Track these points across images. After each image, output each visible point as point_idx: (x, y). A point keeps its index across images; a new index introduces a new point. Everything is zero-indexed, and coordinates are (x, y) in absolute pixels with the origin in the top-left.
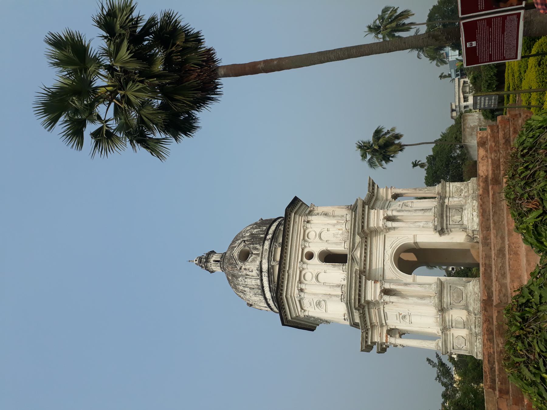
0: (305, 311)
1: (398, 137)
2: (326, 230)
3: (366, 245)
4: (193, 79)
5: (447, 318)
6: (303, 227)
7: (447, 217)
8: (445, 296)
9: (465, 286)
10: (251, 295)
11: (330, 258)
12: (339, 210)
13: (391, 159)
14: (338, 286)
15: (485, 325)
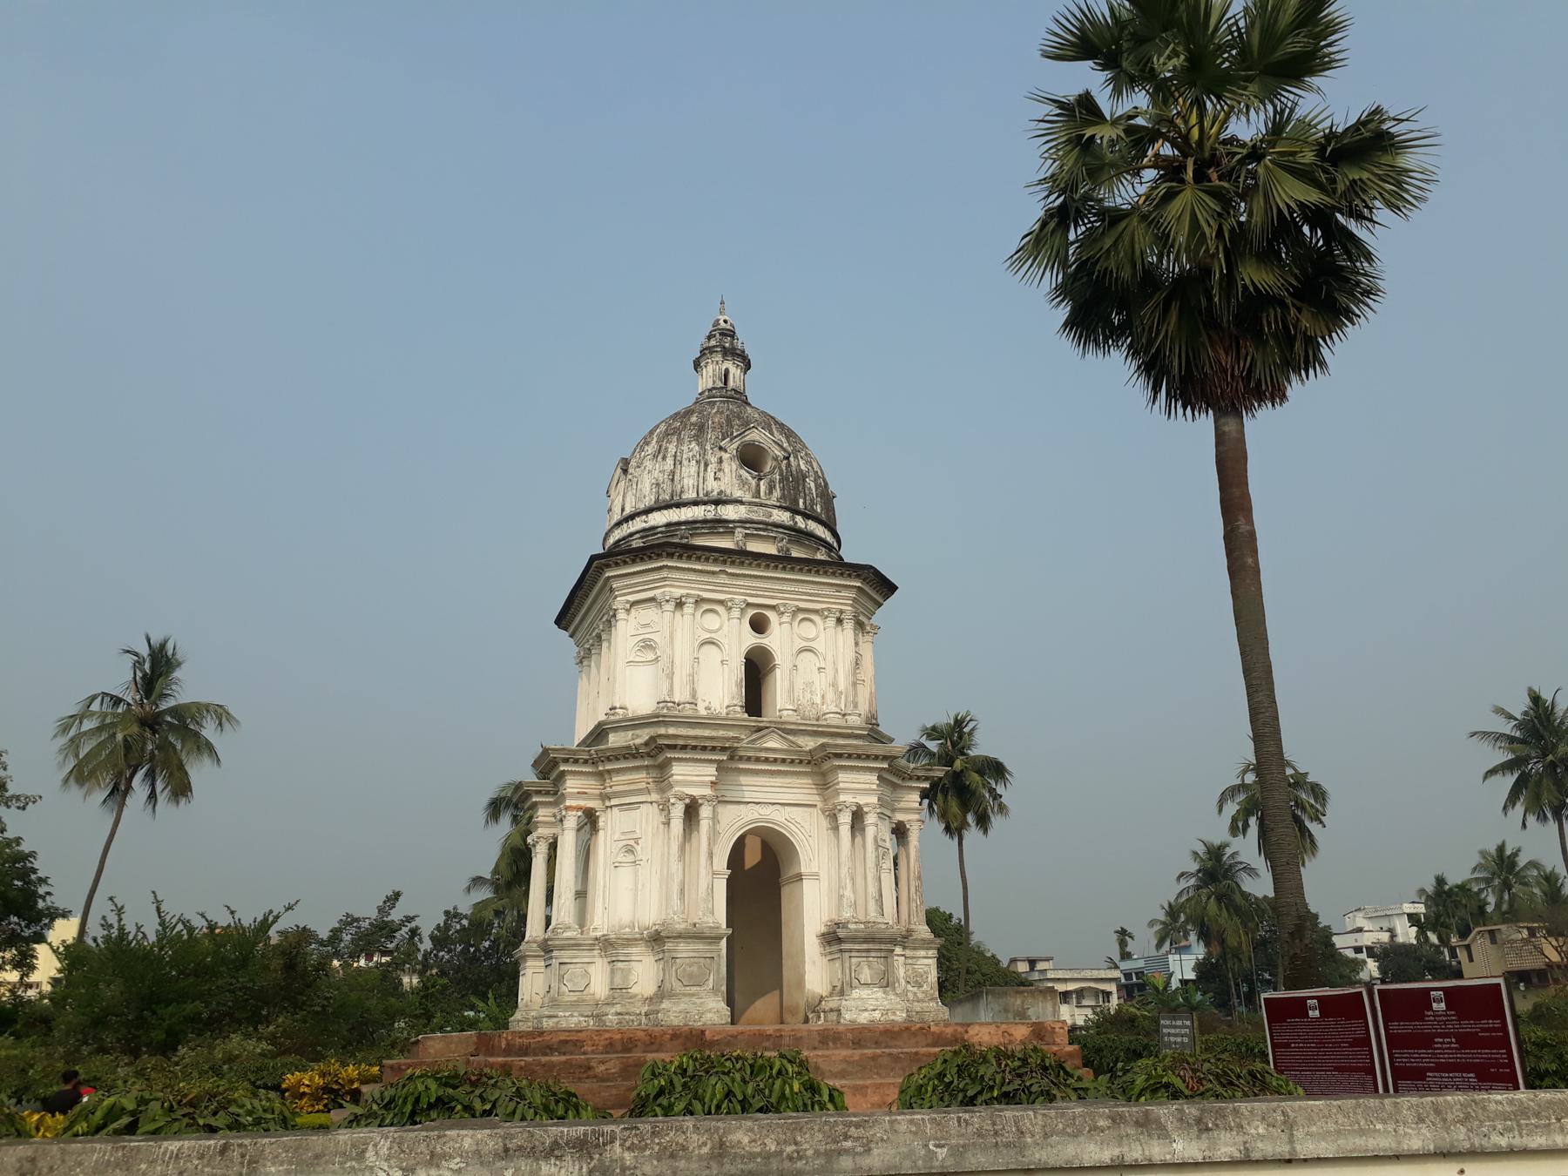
0: (628, 611)
1: (983, 821)
2: (823, 665)
3: (792, 761)
4: (1216, 356)
5: (634, 950)
6: (829, 610)
7: (868, 951)
9: (715, 991)
11: (757, 670)
12: (867, 696)
13: (926, 801)
14: (694, 694)
15: (641, 1035)
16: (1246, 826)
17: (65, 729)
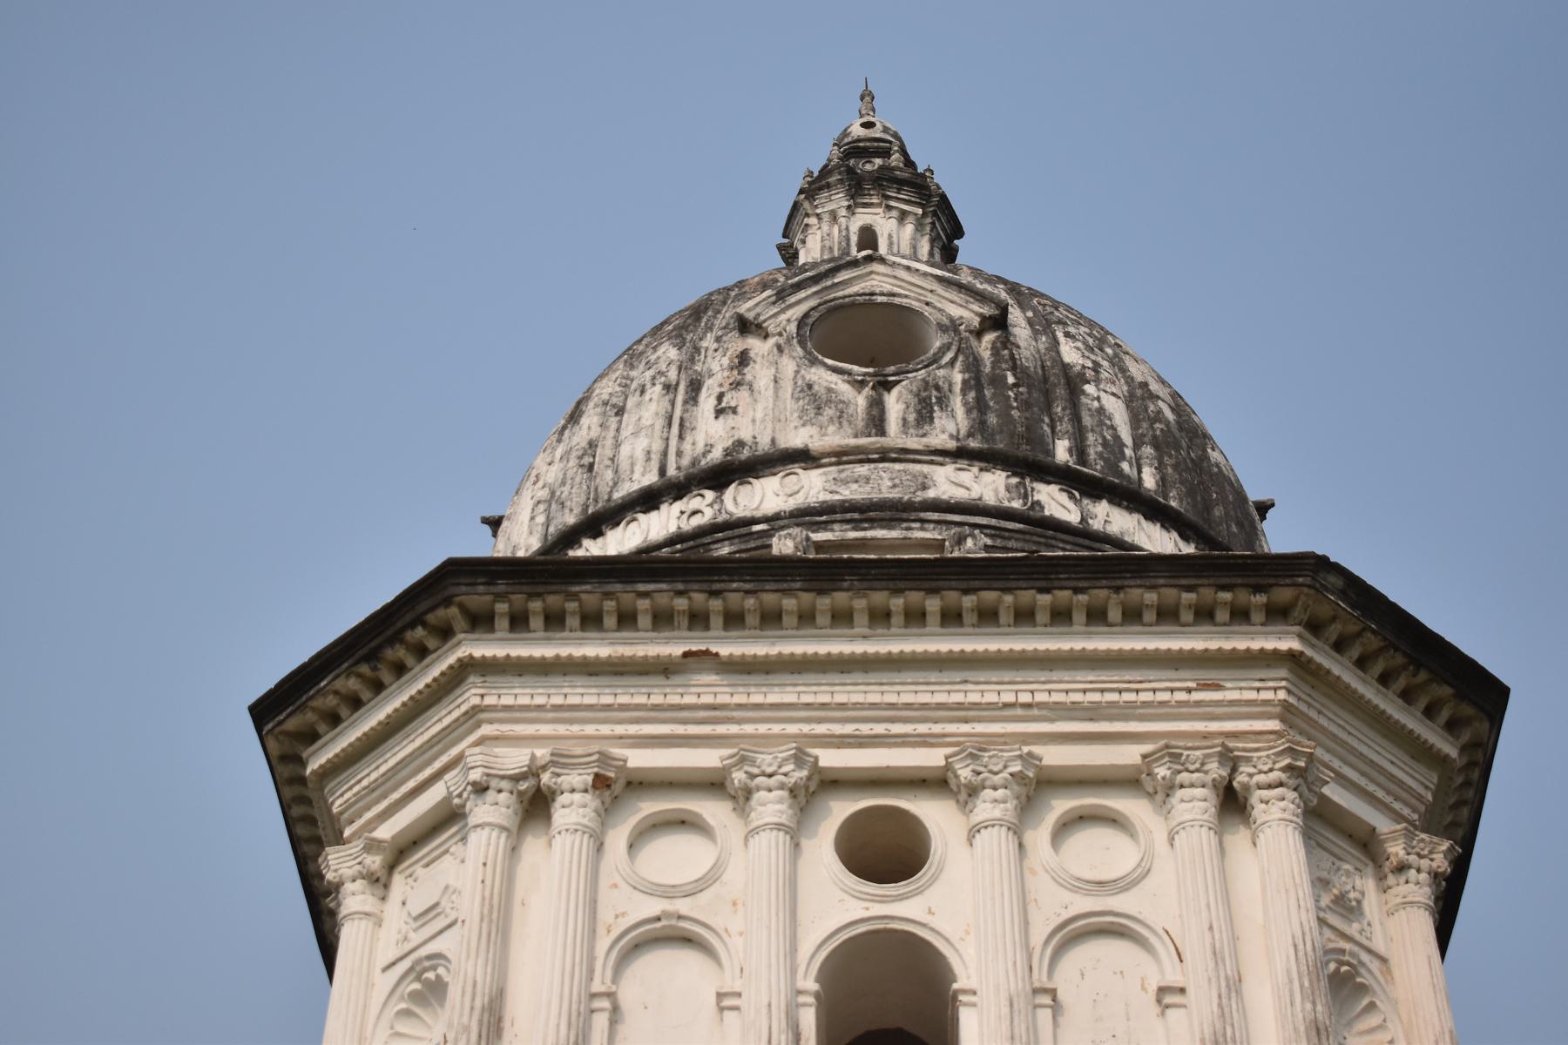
10: (552, 475)
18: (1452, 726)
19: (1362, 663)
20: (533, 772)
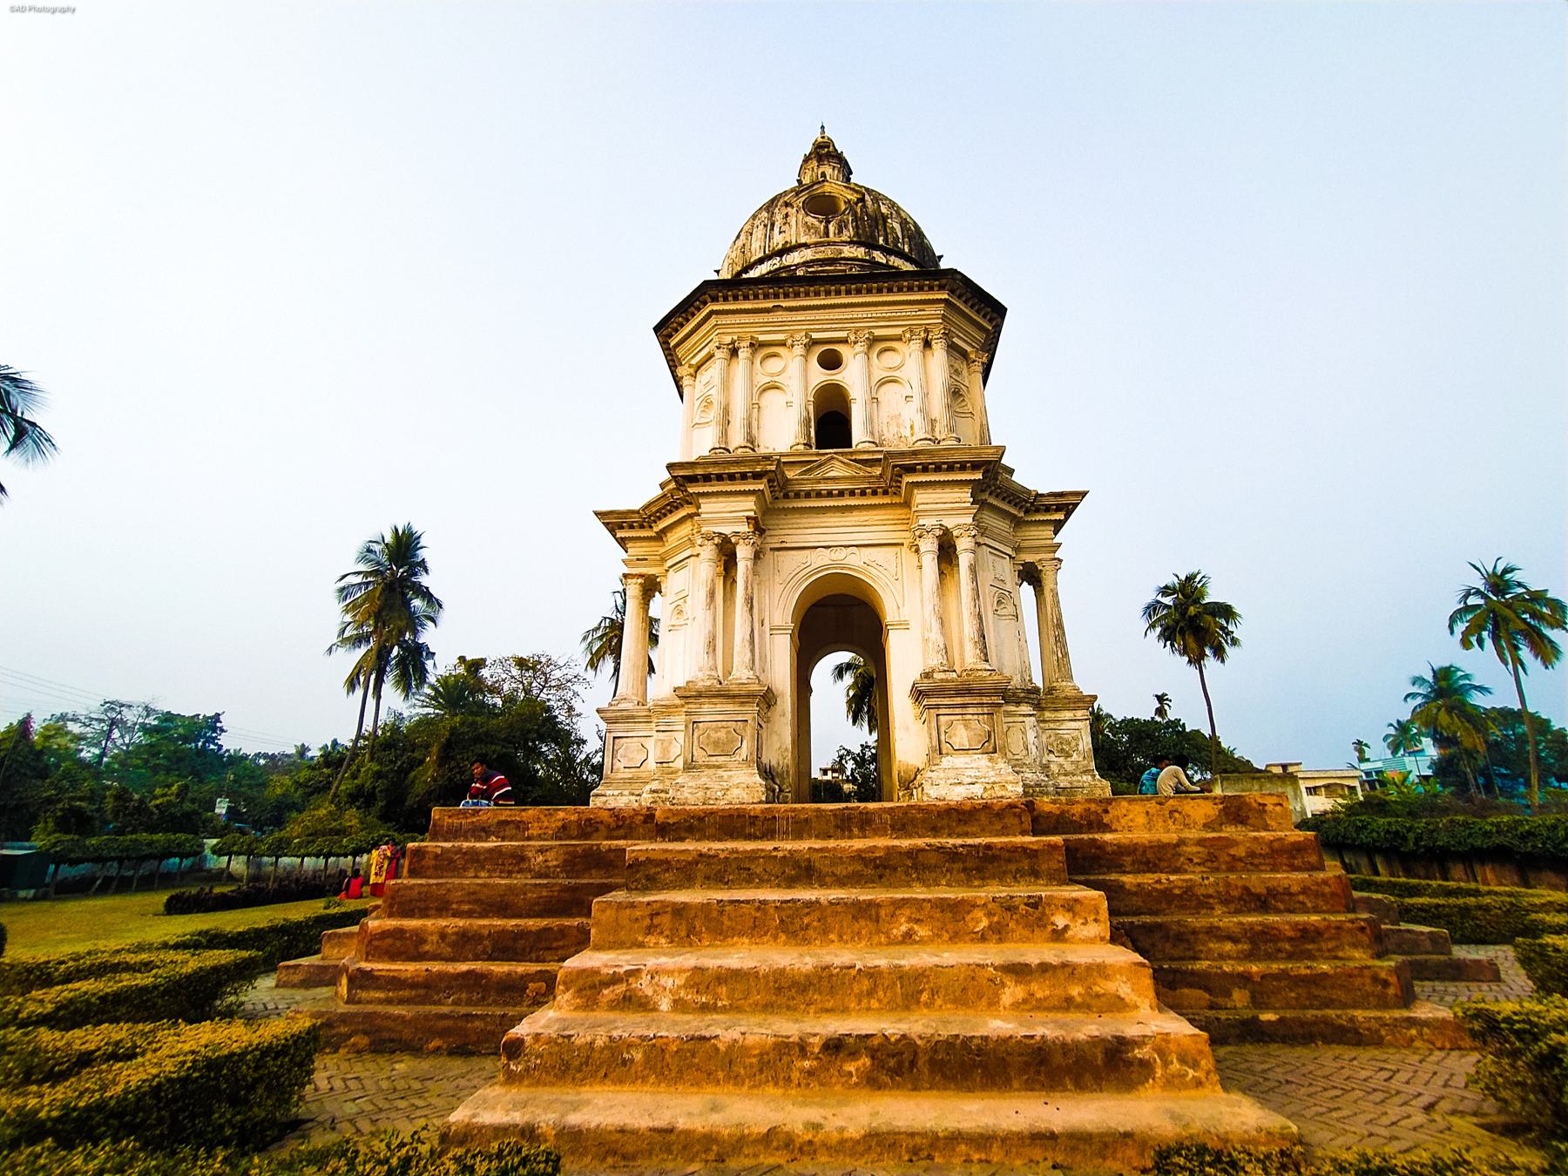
1: (1219, 653)
5: (672, 719)
7: (964, 706)
8: (719, 708)
15: (605, 816)
16: (1480, 642)
17: (585, 638)
18: (990, 321)
19: (965, 302)
20: (733, 342)
